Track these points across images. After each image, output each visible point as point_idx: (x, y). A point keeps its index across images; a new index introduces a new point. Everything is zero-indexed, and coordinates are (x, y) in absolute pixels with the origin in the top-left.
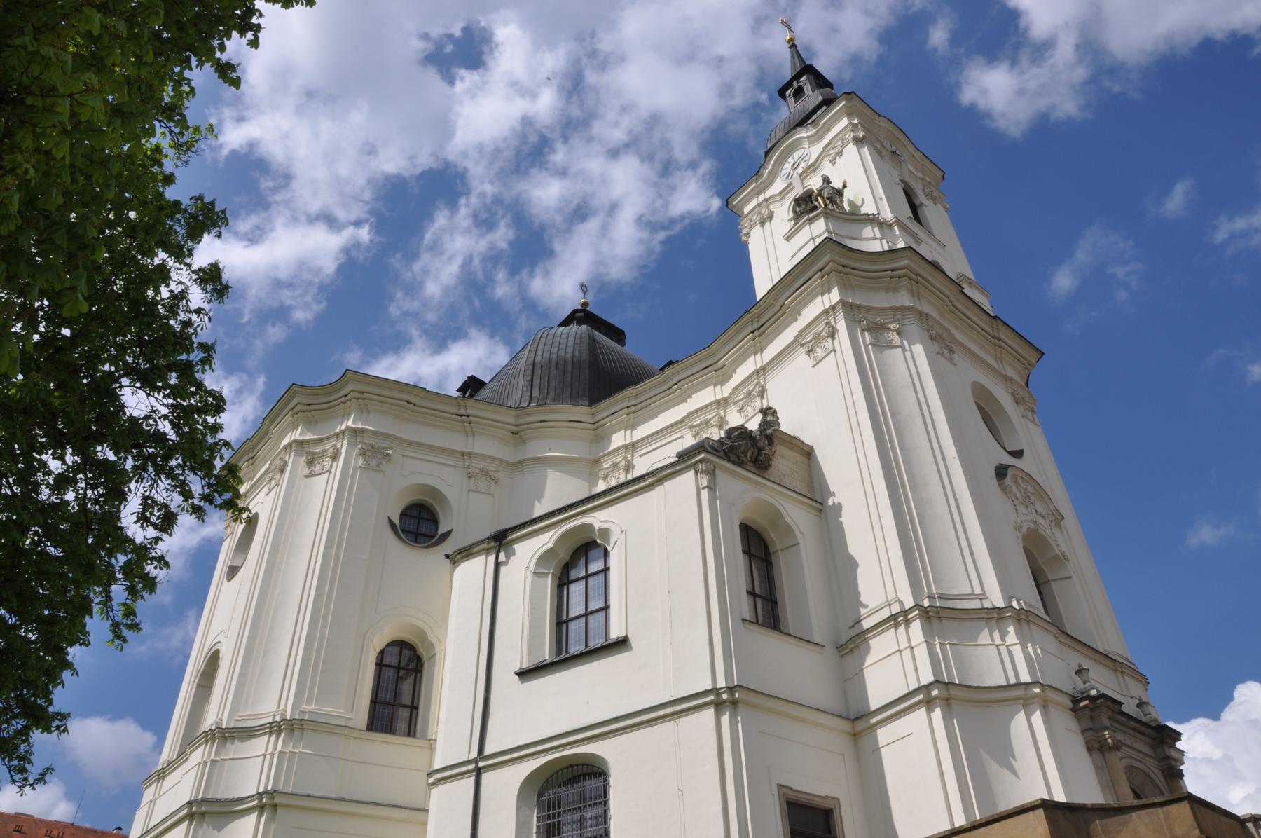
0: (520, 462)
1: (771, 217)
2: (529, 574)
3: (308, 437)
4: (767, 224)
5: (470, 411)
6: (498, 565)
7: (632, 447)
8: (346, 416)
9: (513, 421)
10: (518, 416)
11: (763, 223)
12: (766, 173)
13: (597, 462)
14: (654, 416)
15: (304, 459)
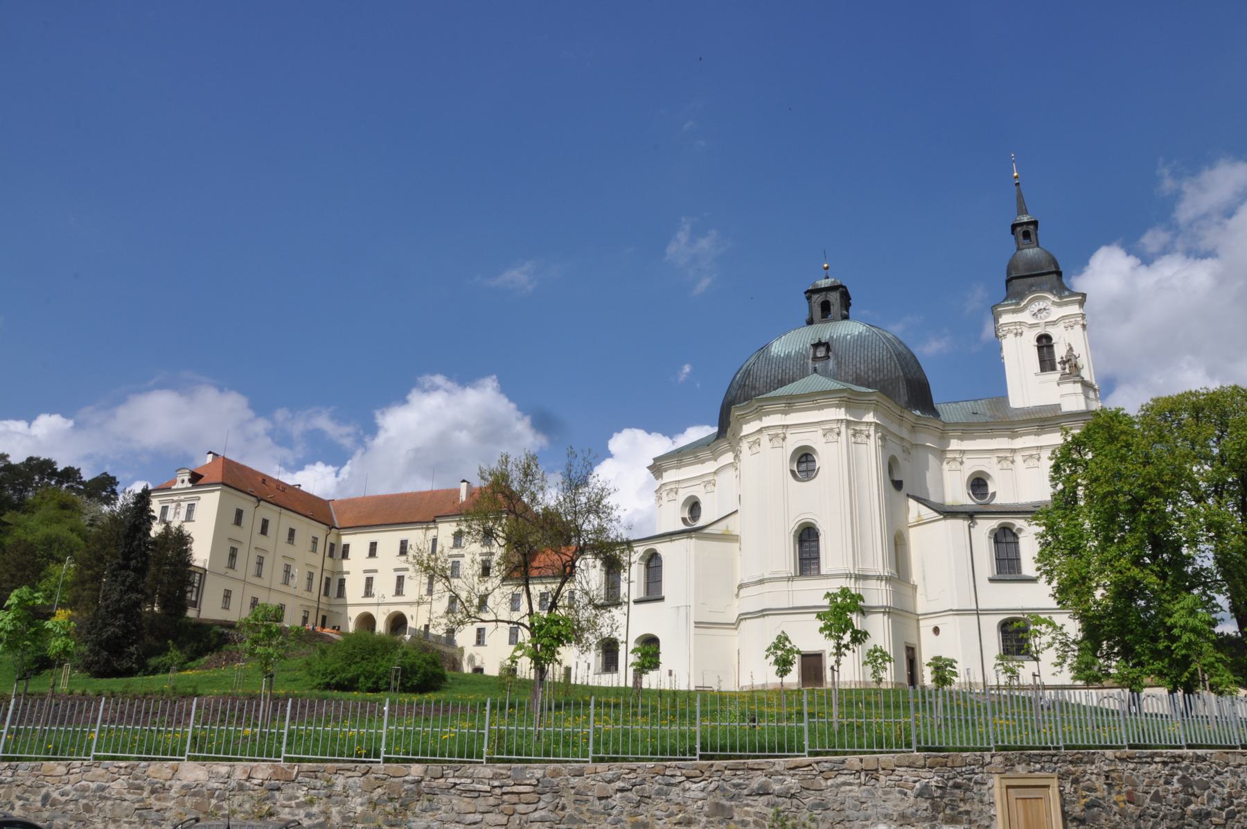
0: (917, 445)
1: (1021, 334)
2: (987, 538)
3: (852, 419)
4: (1018, 337)
5: (905, 415)
6: (969, 527)
7: (963, 452)
8: (867, 411)
9: (913, 420)
10: (916, 419)
11: (1016, 334)
12: (1022, 304)
13: (944, 452)
14: (974, 438)
15: (851, 432)
